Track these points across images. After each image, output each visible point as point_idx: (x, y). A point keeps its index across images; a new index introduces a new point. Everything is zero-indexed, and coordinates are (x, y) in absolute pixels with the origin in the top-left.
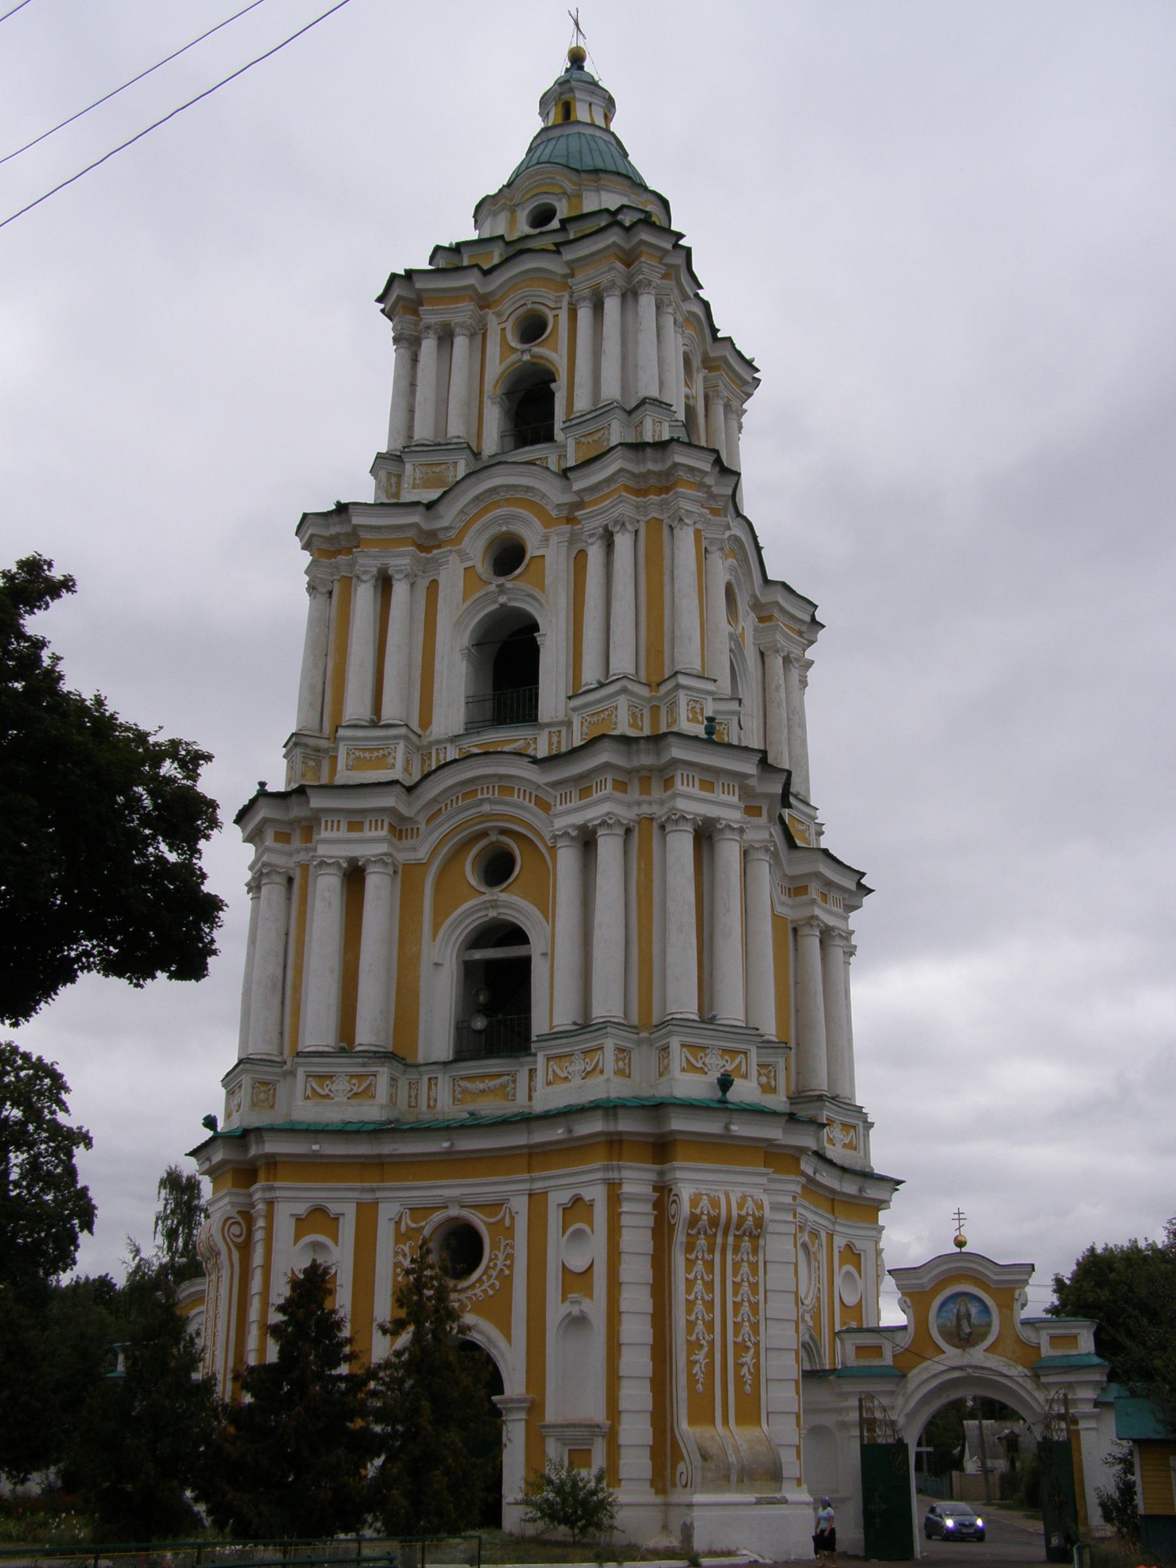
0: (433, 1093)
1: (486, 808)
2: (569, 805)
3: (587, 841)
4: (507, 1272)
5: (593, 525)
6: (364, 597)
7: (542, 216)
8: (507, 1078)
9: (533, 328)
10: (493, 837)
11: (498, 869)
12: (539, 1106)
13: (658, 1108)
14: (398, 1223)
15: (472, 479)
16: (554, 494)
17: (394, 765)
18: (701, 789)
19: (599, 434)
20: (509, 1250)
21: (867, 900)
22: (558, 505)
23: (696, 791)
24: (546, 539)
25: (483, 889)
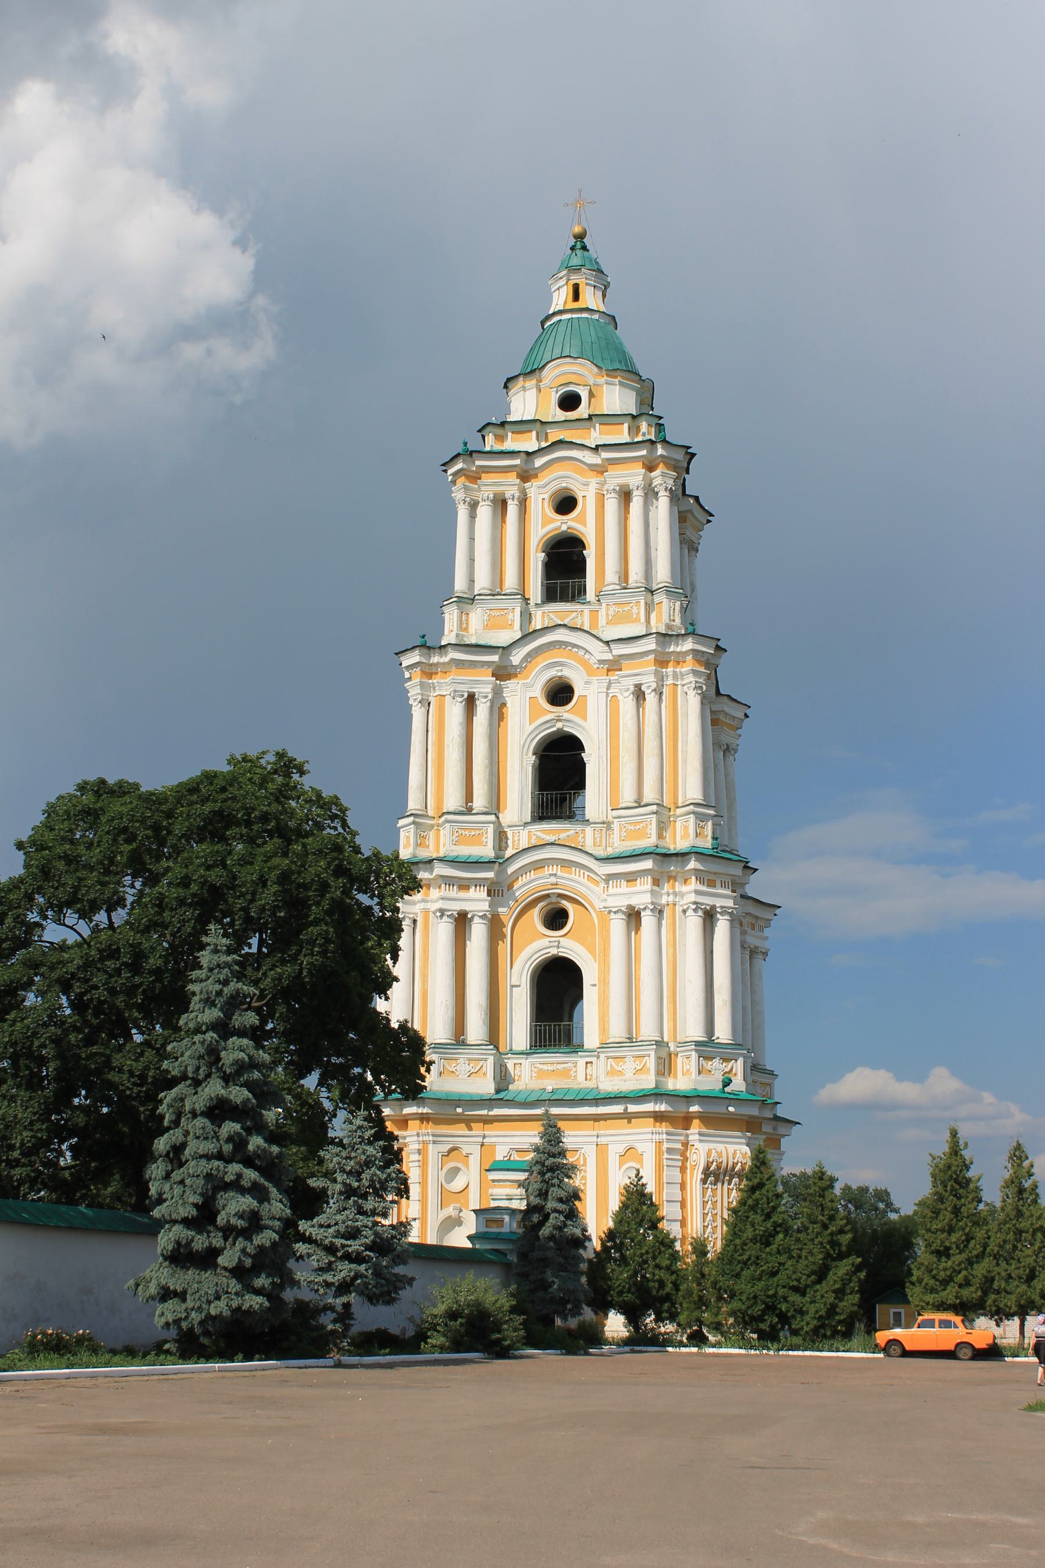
1: (553, 880)
2: (619, 890)
3: (634, 916)
5: (630, 683)
6: (455, 711)
7: (570, 402)
9: (566, 504)
11: (556, 919)
13: (688, 1098)
16: (598, 652)
18: (708, 886)
22: (601, 662)
23: (704, 888)
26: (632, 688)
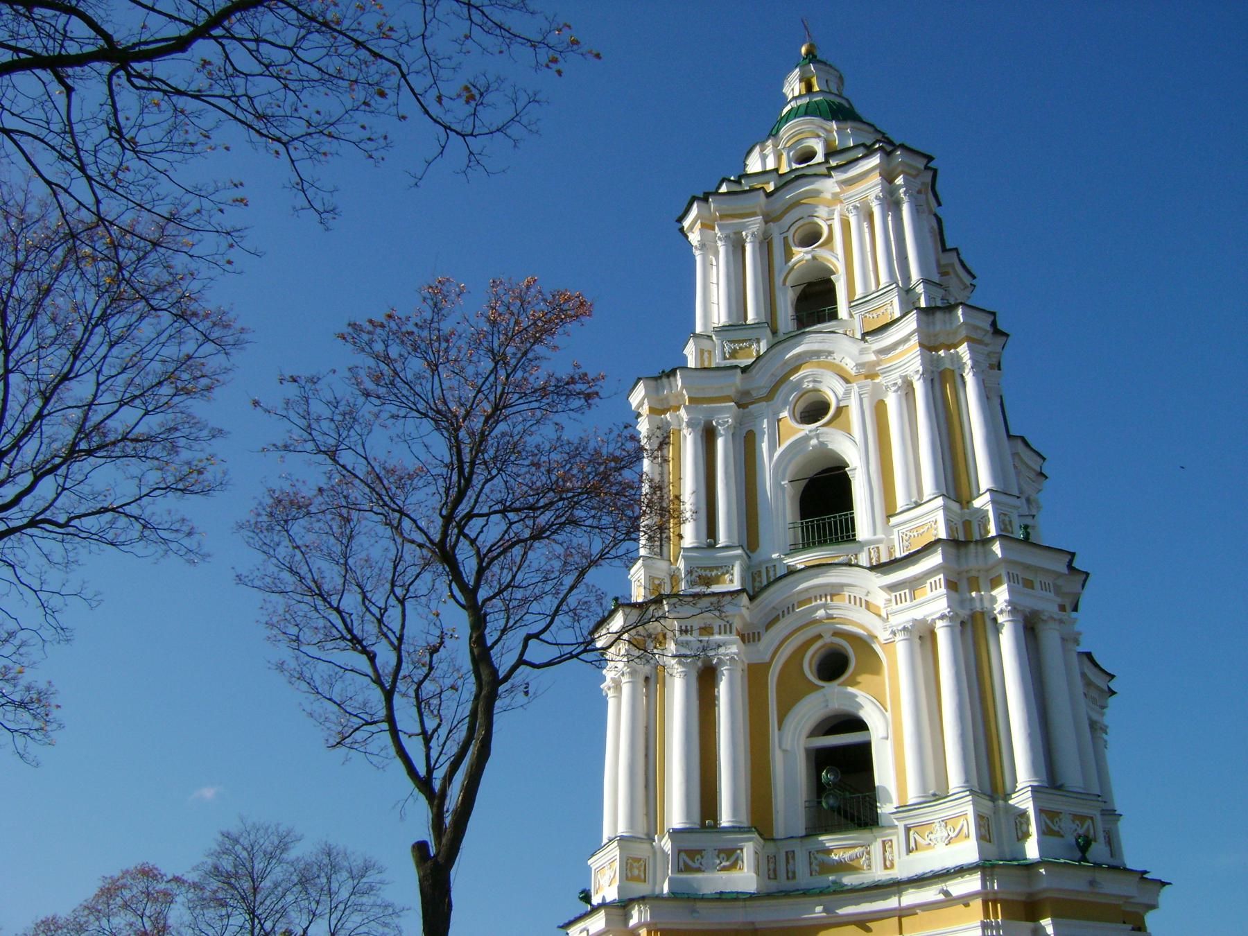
0: (791, 867)
1: (821, 613)
2: (905, 604)
5: (895, 377)
8: (858, 850)
10: (828, 639)
12: (901, 871)
15: (780, 347)
17: (732, 581)
19: (882, 310)
21: (1111, 701)
24: (847, 393)
25: (821, 683)
26: (900, 381)
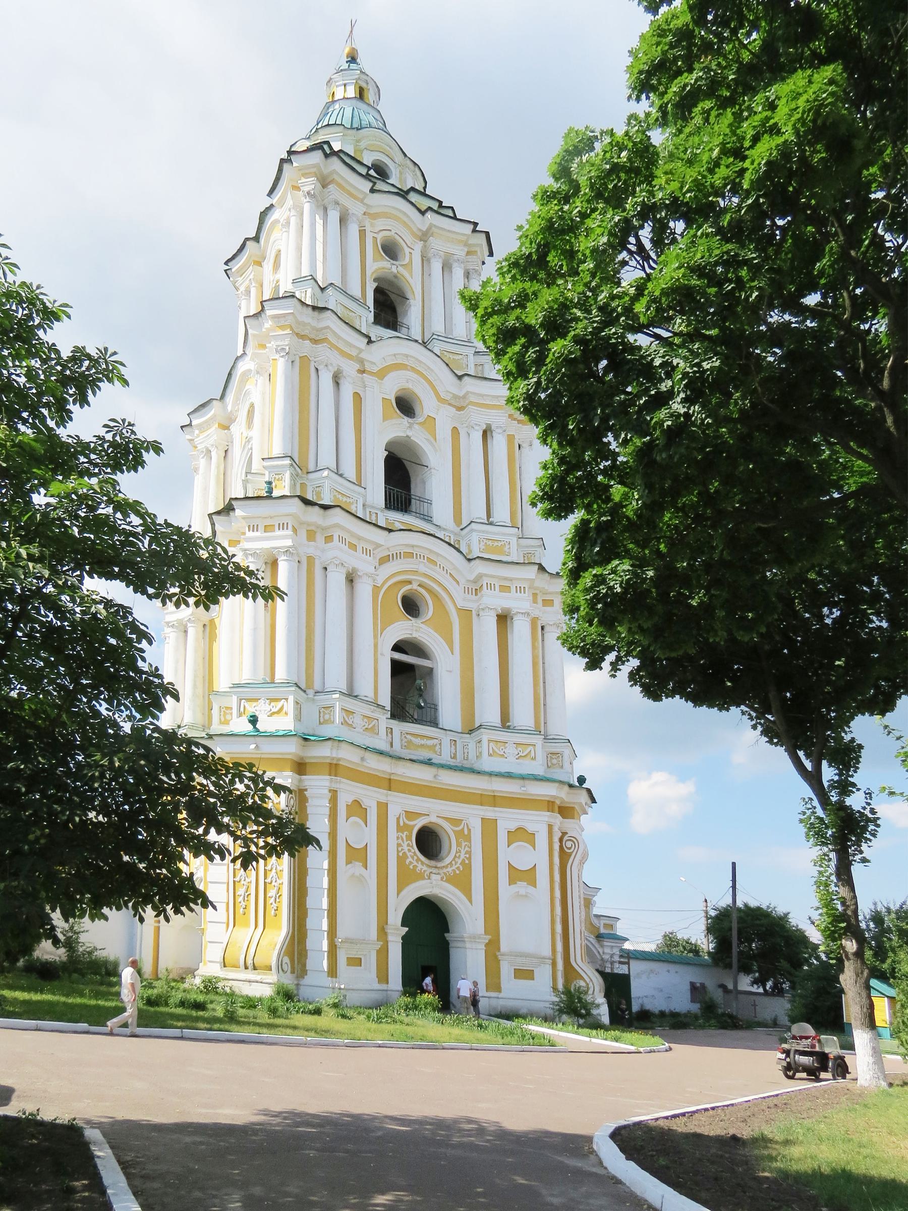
4: (467, 862)
11: (411, 606)
14: (398, 819)
20: (467, 849)
